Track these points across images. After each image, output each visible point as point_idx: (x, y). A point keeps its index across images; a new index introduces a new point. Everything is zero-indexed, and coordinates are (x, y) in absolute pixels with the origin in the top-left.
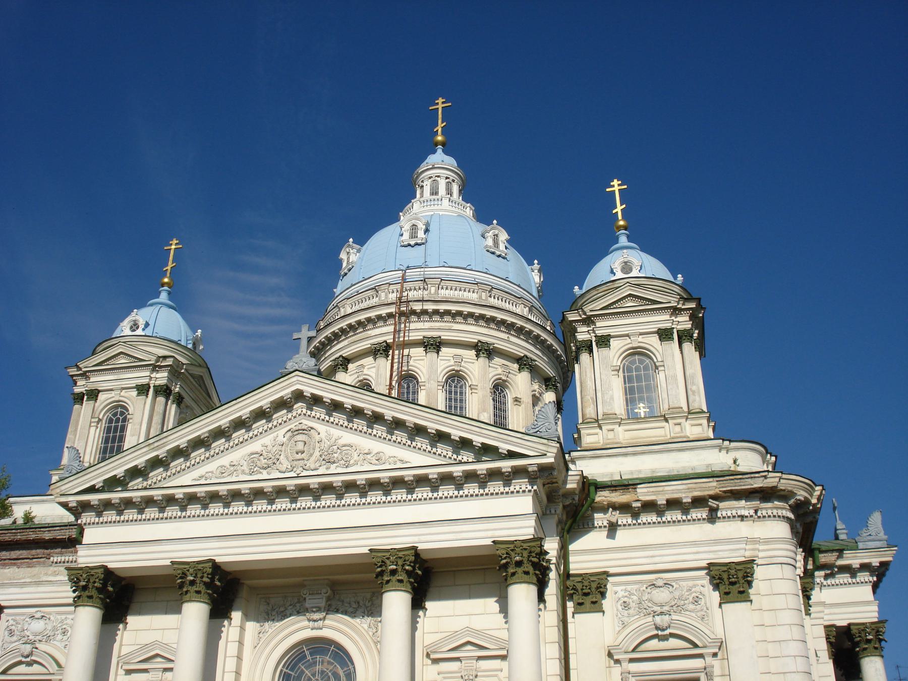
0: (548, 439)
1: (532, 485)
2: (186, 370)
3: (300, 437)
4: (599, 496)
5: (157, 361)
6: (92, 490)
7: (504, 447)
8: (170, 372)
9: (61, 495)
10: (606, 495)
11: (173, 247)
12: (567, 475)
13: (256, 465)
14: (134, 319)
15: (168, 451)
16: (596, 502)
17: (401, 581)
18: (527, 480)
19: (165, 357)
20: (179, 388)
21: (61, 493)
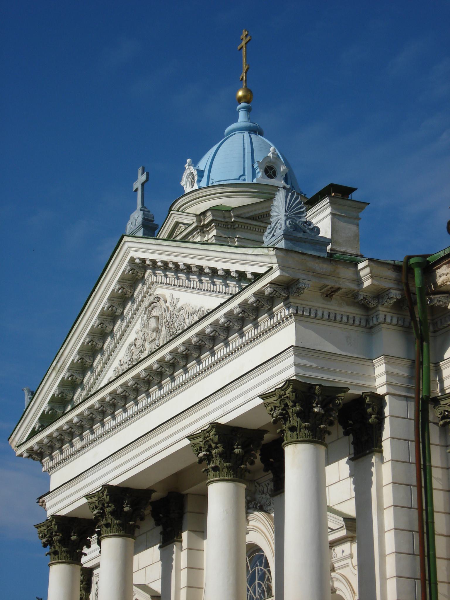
0: (268, 248)
1: (288, 308)
2: (236, 216)
3: (155, 313)
4: (440, 276)
5: (199, 221)
6: (34, 433)
7: (249, 269)
8: (217, 227)
9: (18, 447)
10: (445, 272)
11: (243, 43)
12: (357, 272)
13: (132, 359)
14: (189, 172)
15: (69, 369)
16: (441, 286)
17: (216, 469)
18: (282, 304)
19: (204, 213)
20: (237, 241)
21: (17, 445)
